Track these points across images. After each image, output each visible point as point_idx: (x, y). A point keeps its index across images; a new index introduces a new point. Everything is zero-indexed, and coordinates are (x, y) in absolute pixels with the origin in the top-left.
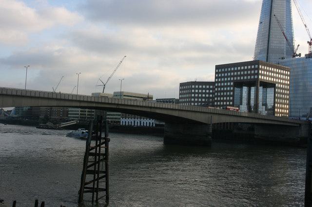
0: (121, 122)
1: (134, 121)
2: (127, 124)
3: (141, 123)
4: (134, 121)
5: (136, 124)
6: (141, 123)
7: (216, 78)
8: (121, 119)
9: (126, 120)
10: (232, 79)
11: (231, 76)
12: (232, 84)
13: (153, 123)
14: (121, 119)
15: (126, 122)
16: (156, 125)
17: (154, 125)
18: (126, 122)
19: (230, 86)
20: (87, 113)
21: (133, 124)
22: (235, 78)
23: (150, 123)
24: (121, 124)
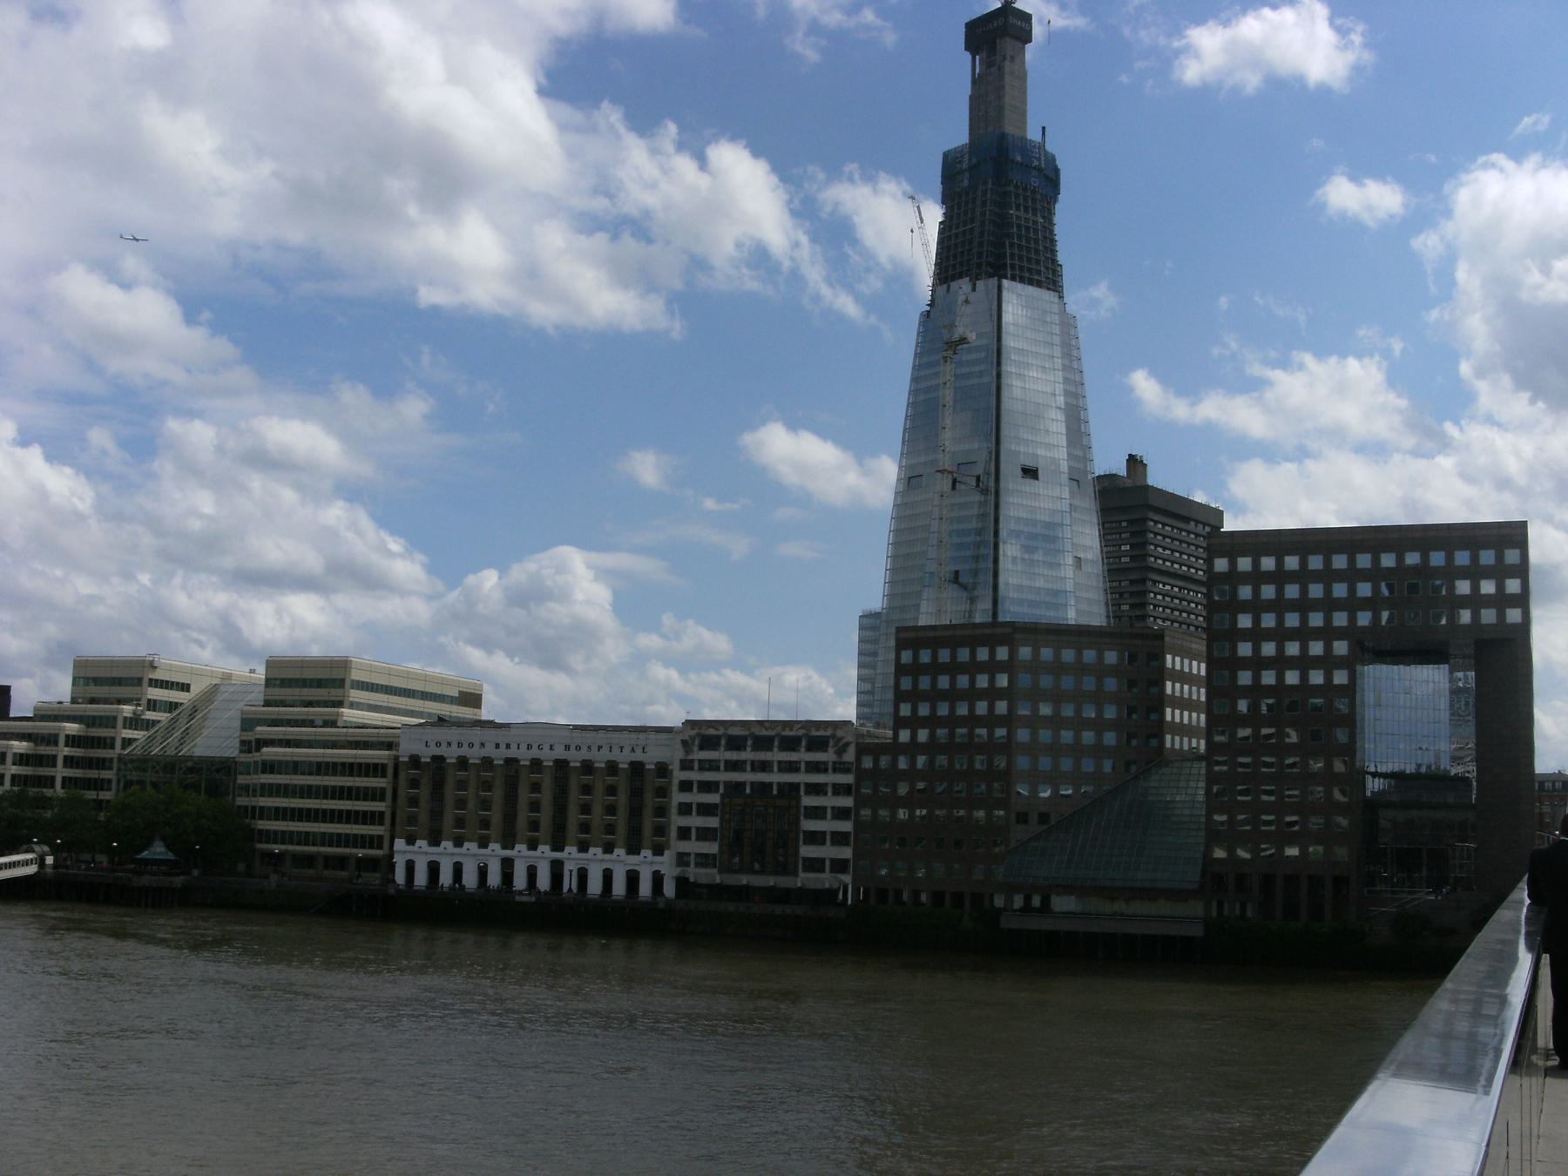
0: (400, 862)
1: (507, 864)
2: (446, 878)
4: (507, 864)
5: (520, 881)
8: (400, 844)
10: (1340, 619)
11: (1329, 605)
12: (1341, 648)
13: (658, 879)
14: (400, 844)
15: (434, 869)
16: (681, 882)
17: (669, 890)
18: (434, 869)
19: (1328, 662)
20: (60, 772)
22: (1364, 619)
23: (633, 878)
24: (400, 876)
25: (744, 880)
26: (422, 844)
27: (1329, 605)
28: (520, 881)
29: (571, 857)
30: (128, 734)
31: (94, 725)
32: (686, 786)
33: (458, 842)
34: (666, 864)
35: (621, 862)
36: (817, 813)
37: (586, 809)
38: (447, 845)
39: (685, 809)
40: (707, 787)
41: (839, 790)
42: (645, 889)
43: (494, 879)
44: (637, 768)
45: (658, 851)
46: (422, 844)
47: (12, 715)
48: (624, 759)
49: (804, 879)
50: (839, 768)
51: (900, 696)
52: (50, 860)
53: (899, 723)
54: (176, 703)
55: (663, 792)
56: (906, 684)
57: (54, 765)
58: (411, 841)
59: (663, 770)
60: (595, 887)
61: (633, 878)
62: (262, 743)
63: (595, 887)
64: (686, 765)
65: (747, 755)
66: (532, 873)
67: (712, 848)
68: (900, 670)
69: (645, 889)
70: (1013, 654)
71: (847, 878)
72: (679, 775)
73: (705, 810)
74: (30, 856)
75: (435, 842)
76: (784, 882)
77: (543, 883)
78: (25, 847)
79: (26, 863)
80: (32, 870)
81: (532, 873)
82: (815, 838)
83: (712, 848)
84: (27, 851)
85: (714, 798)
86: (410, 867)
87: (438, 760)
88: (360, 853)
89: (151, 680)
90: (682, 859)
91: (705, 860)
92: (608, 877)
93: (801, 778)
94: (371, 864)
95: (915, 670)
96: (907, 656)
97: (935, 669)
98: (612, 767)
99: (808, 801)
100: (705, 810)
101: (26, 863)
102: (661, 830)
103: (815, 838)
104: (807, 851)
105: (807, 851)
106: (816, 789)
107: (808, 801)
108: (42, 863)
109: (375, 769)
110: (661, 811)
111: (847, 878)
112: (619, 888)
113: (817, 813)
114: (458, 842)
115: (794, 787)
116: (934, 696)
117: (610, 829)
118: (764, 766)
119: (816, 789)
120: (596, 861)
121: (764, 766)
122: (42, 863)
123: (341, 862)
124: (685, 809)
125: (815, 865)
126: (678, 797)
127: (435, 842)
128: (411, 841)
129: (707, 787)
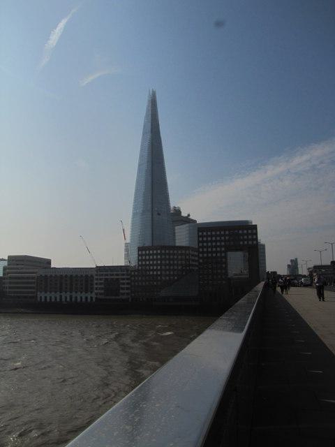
1: (61, 296)
3: (71, 299)
4: (61, 296)
5: (63, 300)
6: (71, 299)
7: (199, 242)
8: (38, 293)
9: (46, 295)
12: (223, 249)
13: (92, 298)
16: (96, 298)
18: (46, 297)
19: (221, 252)
21: (58, 300)
23: (86, 298)
24: (39, 299)
25: (108, 297)
26: (43, 293)
27: (221, 241)
28: (63, 300)
29: (74, 294)
32: (97, 279)
33: (51, 292)
34: (94, 296)
35: (84, 295)
36: (124, 284)
37: (76, 284)
38: (48, 293)
39: (96, 284)
40: (101, 279)
41: (127, 279)
42: (89, 300)
43: (58, 300)
44: (87, 276)
45: (91, 292)
46: (43, 293)
48: (84, 275)
49: (121, 297)
50: (128, 275)
51: (139, 260)
53: (139, 265)
55: (92, 281)
56: (140, 258)
58: (41, 292)
59: (92, 276)
60: (79, 300)
61: (86, 298)
62: (8, 273)
63: (79, 300)
64: (96, 275)
65: (109, 273)
66: (66, 298)
67: (103, 291)
68: (139, 255)
69: (89, 300)
70: (161, 252)
71: (129, 296)
72: (95, 277)
73: (101, 284)
75: (46, 292)
76: (117, 297)
77: (68, 299)
81: (66, 298)
82: (123, 289)
83: (103, 291)
85: (102, 281)
86: (41, 297)
87: (46, 276)
88: (30, 295)
90: (96, 294)
91: (101, 294)
92: (81, 298)
93: (120, 277)
94: (33, 297)
95: (142, 255)
96: (140, 253)
97: (146, 255)
98: (82, 276)
99: (122, 281)
100: (101, 284)
102: (92, 288)
103: (123, 289)
104: (121, 291)
105: (121, 291)
106: (124, 279)
107: (122, 281)
109: (33, 278)
110: (92, 285)
111: (129, 296)
112: (84, 300)
113: (124, 284)
114: (51, 292)
115: (117, 279)
116: (145, 260)
117: (82, 288)
118: (111, 275)
119: (124, 279)
120: (79, 295)
121: (111, 275)
123: (25, 297)
124: (96, 284)
125: (123, 294)
126: (95, 282)
127: (46, 292)
128: (41, 292)
129: (101, 279)
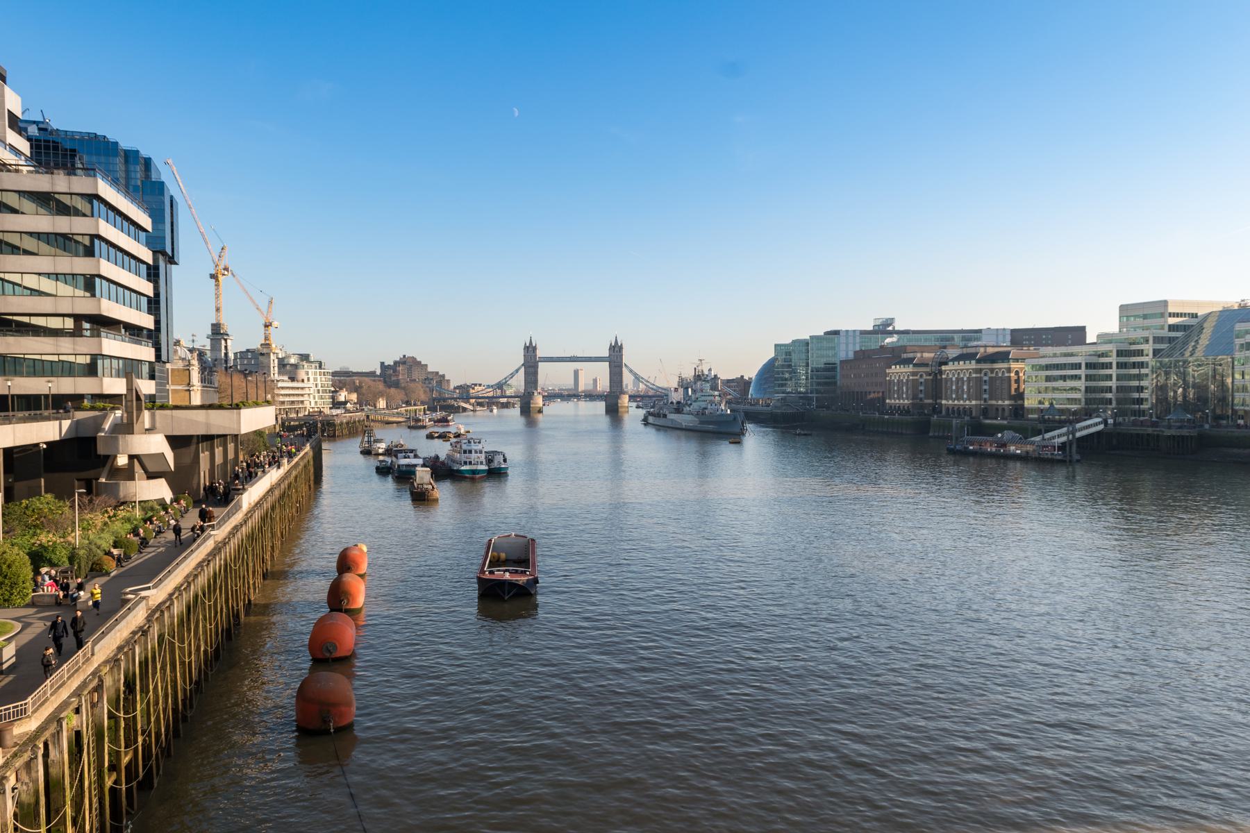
20: (1113, 371)
30: (1158, 346)
31: (1134, 344)
47: (1087, 342)
52: (1110, 421)
54: (1189, 326)
57: (1118, 363)
74: (1099, 420)
78: (1095, 415)
79: (1096, 424)
80: (1101, 427)
84: (1097, 417)
89: (1170, 314)
101: (1096, 424)
108: (1105, 422)
122: (1105, 422)
